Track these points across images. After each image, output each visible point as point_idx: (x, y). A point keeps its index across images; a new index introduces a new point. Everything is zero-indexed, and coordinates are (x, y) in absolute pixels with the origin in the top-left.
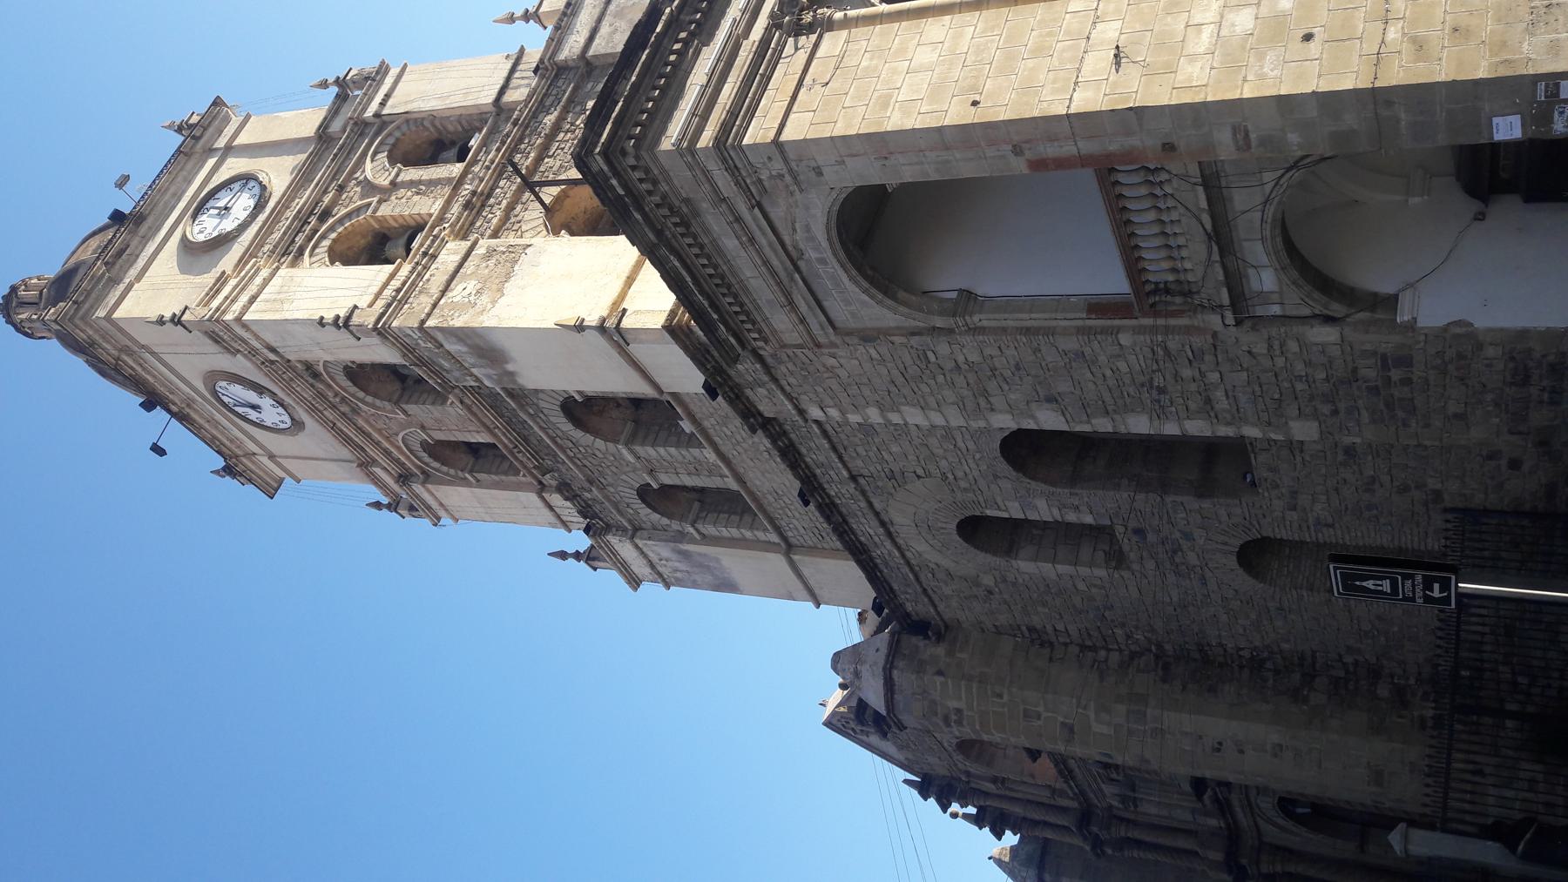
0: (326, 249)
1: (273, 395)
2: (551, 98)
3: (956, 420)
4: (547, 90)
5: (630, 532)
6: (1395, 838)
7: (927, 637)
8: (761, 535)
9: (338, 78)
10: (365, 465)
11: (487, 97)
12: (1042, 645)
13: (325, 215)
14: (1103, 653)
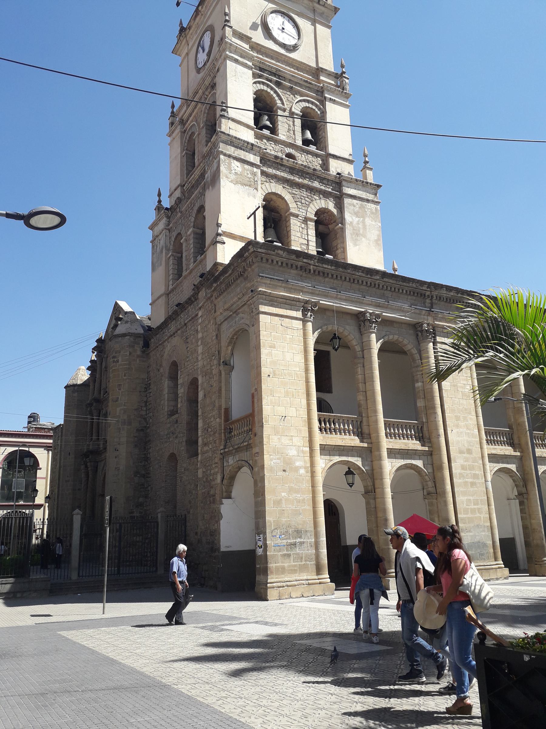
0: (262, 88)
1: (208, 61)
2: (326, 183)
3: (200, 364)
4: (330, 180)
5: (167, 228)
6: (77, 511)
7: (143, 347)
8: (171, 282)
9: (344, 73)
10: (186, 101)
11: (332, 150)
12: (145, 388)
13: (278, 84)
14: (145, 409)
